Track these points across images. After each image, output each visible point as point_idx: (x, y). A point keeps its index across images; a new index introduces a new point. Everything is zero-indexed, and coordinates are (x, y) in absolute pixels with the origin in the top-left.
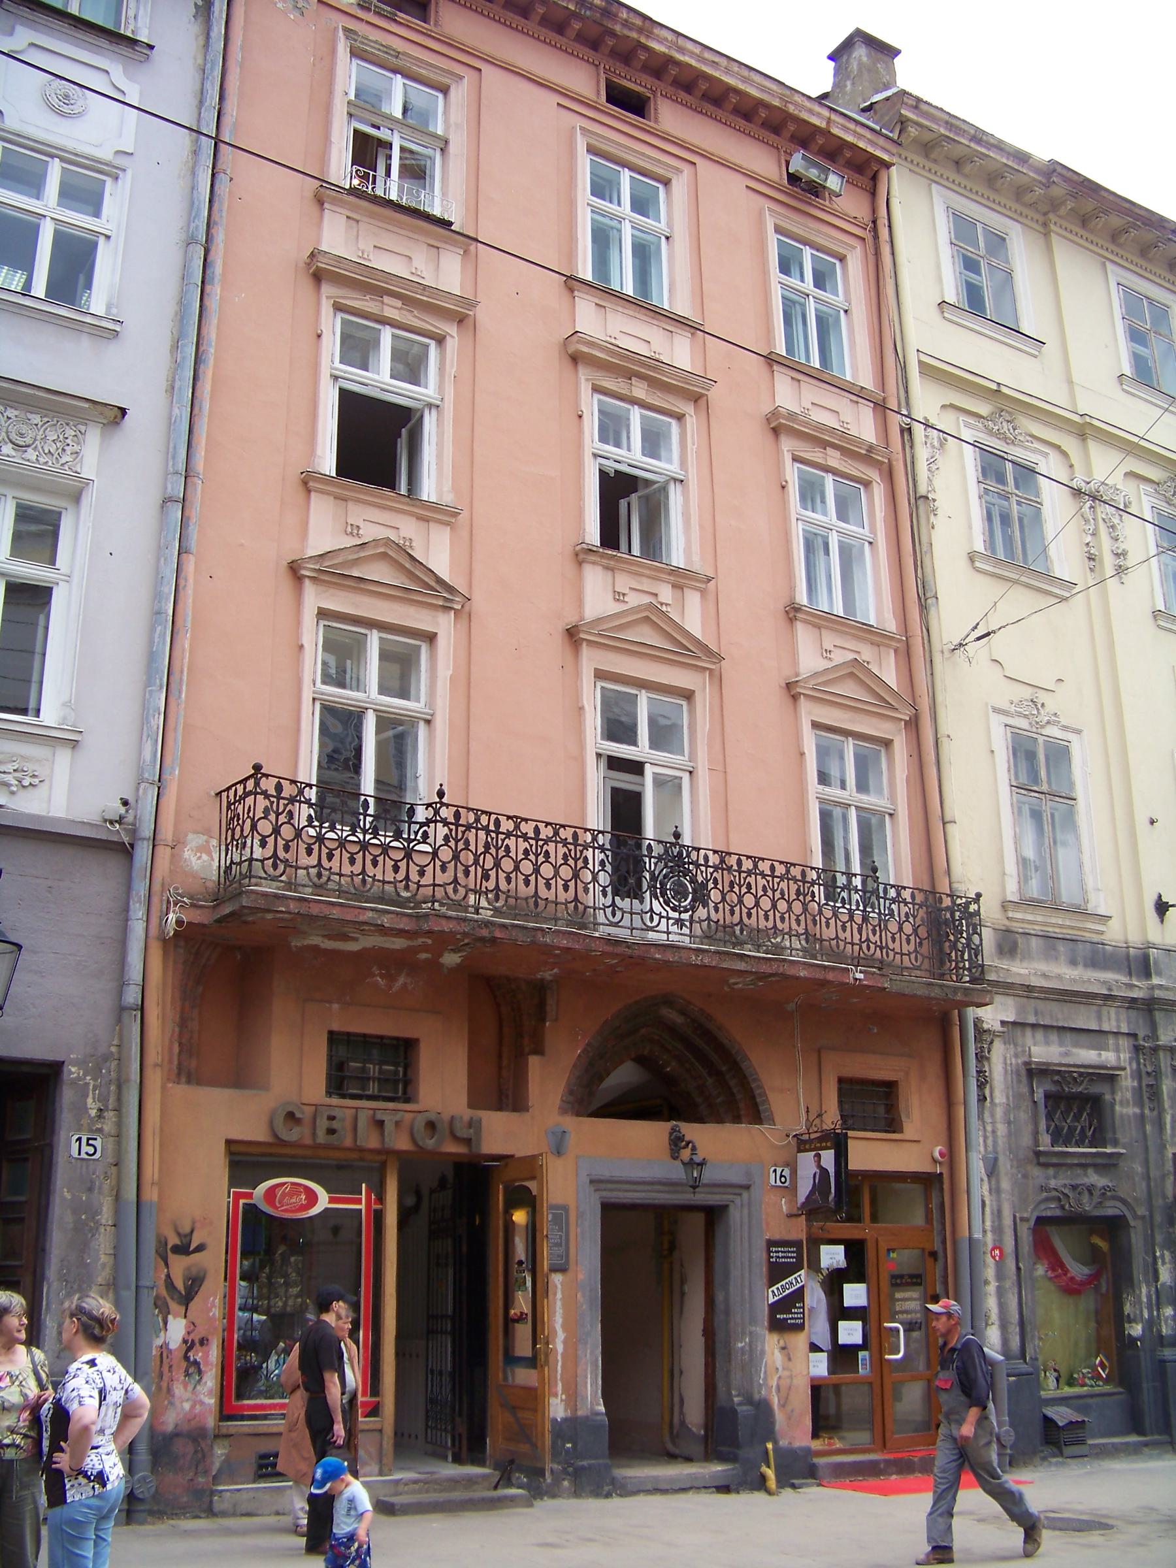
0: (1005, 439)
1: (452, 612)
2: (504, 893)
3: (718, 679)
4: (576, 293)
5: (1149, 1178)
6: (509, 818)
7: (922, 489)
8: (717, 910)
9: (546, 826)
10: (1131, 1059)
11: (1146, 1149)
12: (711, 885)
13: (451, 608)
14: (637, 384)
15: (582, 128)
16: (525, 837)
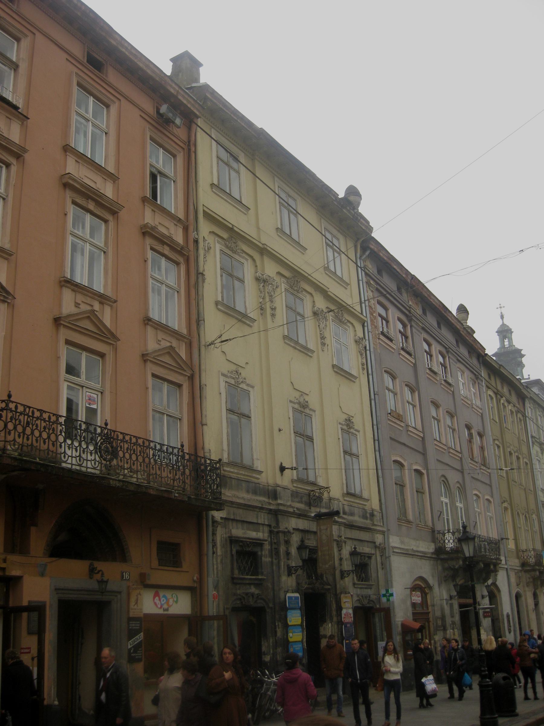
0: (232, 250)
1: (6, 304)
2: (35, 447)
3: (116, 350)
4: (68, 153)
5: (273, 589)
6: (38, 410)
7: (201, 270)
8: (121, 461)
9: (53, 416)
10: (268, 536)
11: (273, 577)
12: (119, 449)
13: (6, 302)
14: (91, 203)
15: (76, 73)
16: (44, 420)
